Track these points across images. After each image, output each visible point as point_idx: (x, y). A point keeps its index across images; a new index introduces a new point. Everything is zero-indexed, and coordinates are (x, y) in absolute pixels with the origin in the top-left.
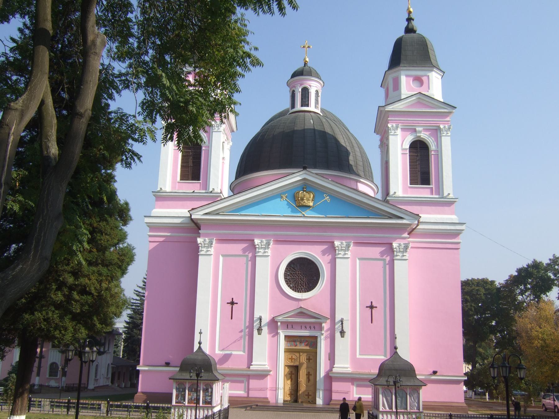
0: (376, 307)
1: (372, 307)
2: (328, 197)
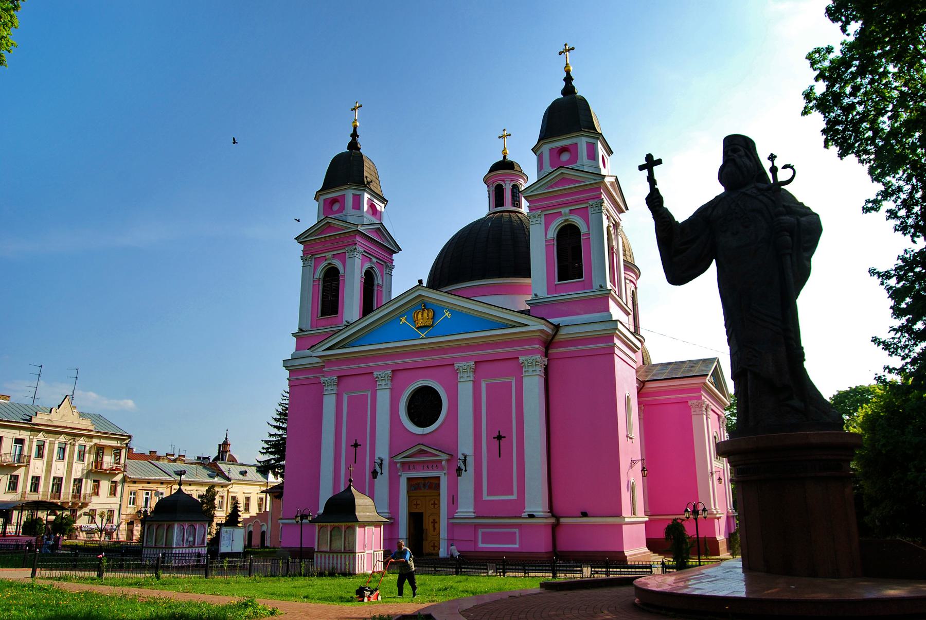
0: (504, 437)
1: (499, 438)
2: (449, 312)
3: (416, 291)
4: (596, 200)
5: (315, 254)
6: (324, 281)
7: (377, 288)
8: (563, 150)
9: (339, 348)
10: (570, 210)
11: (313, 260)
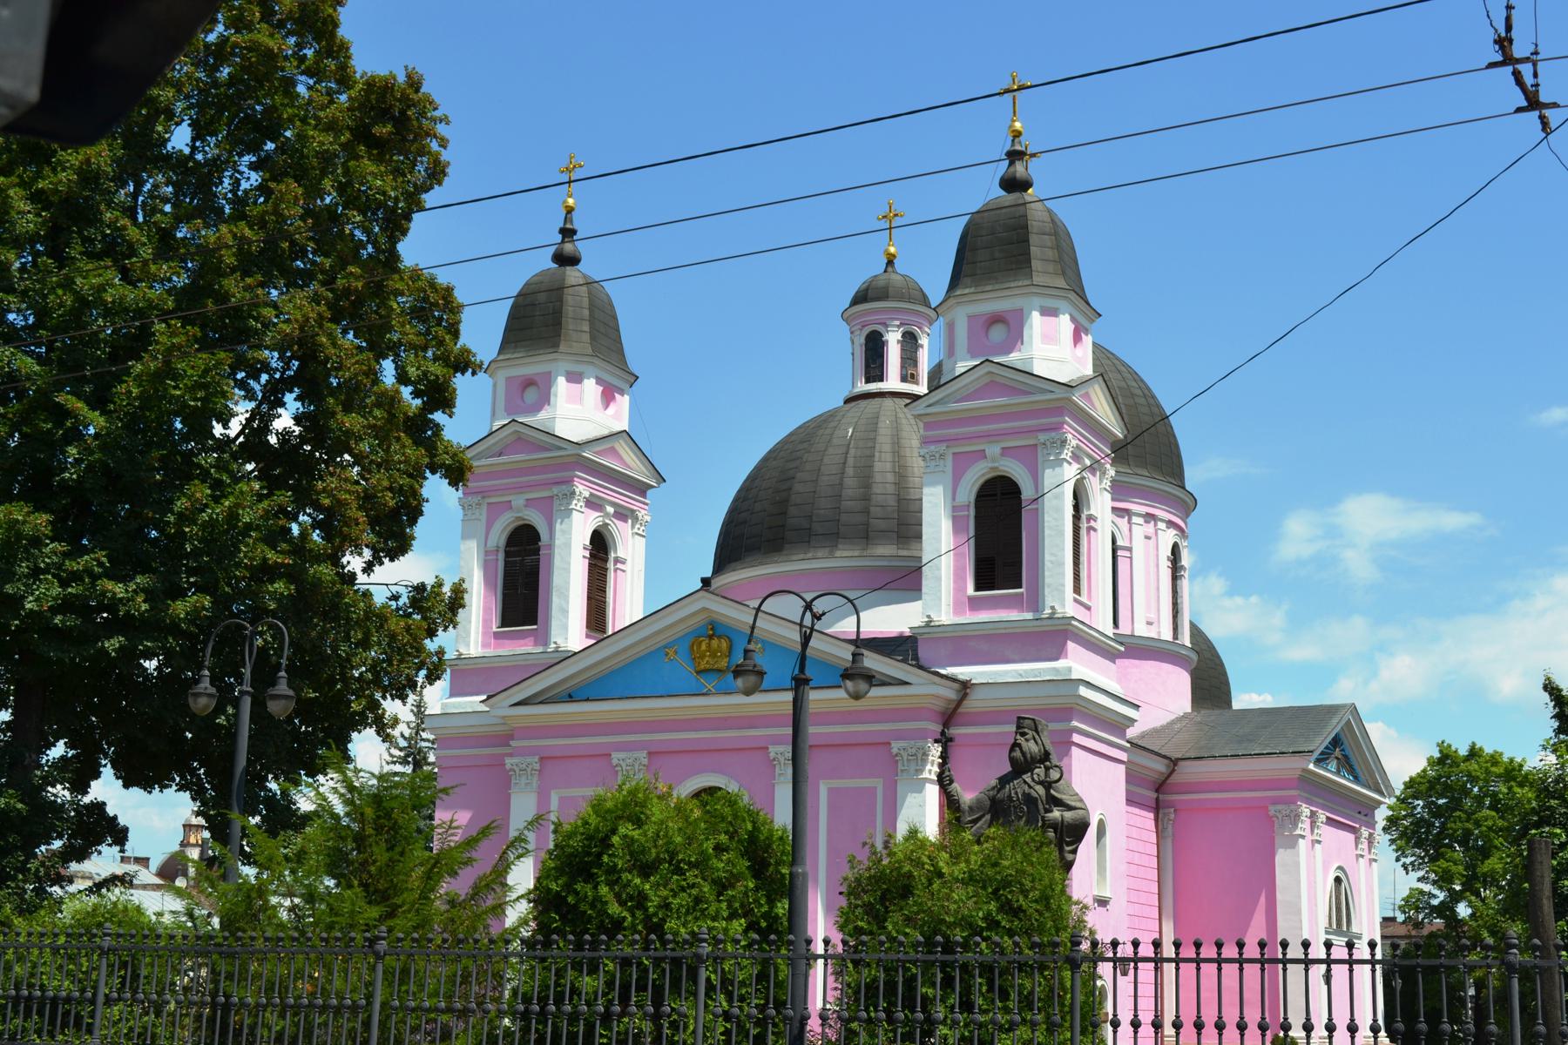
3: (698, 600)
4: (1053, 434)
5: (489, 497)
6: (508, 554)
7: (615, 564)
8: (996, 319)
9: (541, 703)
10: (1003, 448)
11: (485, 507)
